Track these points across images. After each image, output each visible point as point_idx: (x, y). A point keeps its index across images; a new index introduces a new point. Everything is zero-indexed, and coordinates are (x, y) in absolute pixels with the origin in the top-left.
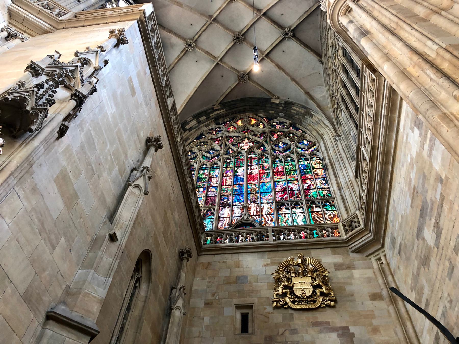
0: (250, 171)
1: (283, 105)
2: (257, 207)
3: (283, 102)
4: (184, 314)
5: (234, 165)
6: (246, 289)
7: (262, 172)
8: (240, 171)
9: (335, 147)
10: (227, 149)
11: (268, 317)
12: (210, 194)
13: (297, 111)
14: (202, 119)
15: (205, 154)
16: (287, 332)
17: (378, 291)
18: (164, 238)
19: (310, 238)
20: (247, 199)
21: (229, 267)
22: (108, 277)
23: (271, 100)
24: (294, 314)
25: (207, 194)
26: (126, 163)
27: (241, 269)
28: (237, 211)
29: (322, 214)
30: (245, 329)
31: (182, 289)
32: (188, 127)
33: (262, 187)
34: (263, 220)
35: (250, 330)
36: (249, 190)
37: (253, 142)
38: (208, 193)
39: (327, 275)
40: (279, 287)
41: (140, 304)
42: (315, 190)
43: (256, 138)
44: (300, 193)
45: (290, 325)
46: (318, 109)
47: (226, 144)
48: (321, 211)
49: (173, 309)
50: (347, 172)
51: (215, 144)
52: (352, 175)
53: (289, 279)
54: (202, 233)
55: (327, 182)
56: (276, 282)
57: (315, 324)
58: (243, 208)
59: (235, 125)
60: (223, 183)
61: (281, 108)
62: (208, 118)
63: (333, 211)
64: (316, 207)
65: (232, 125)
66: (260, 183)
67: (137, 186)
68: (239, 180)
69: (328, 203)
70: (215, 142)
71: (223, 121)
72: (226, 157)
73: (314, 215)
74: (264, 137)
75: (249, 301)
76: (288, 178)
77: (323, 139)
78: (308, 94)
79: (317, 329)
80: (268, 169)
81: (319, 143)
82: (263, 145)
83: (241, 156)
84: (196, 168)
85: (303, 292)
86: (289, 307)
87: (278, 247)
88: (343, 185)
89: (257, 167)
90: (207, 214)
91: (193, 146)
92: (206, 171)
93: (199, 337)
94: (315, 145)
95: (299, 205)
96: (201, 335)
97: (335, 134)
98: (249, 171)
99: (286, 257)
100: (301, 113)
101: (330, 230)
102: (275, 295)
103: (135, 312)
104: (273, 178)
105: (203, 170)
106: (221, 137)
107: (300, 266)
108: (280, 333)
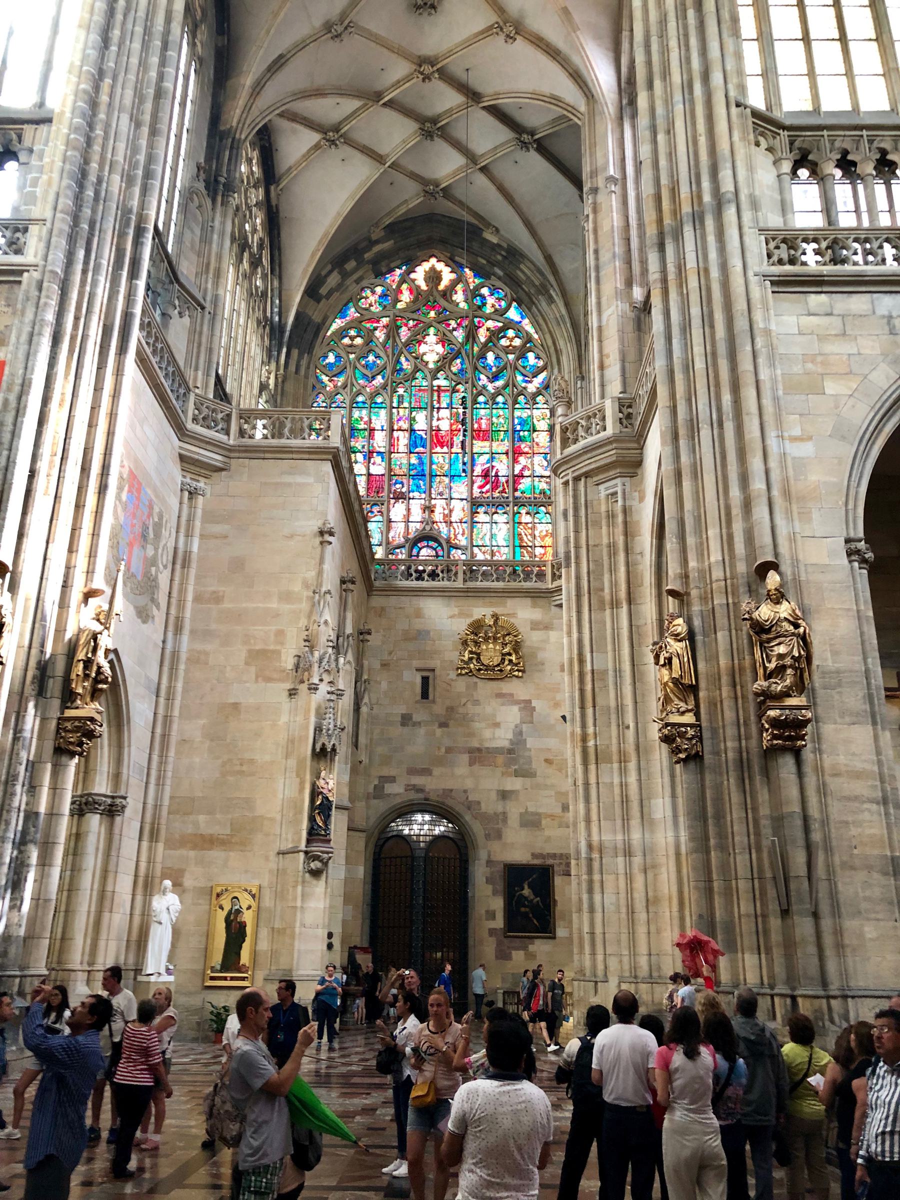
1: (503, 253)
5: (410, 403)
7: (454, 427)
13: (528, 278)
21: (407, 617)
30: (425, 695)
32: (323, 291)
38: (371, 466)
57: (500, 695)
61: (499, 258)
62: (360, 263)
64: (527, 513)
68: (418, 441)
69: (542, 508)
71: (388, 265)
73: (521, 530)
75: (430, 664)
78: (549, 259)
79: (499, 700)
92: (364, 412)
94: (544, 368)
98: (435, 423)
100: (534, 285)
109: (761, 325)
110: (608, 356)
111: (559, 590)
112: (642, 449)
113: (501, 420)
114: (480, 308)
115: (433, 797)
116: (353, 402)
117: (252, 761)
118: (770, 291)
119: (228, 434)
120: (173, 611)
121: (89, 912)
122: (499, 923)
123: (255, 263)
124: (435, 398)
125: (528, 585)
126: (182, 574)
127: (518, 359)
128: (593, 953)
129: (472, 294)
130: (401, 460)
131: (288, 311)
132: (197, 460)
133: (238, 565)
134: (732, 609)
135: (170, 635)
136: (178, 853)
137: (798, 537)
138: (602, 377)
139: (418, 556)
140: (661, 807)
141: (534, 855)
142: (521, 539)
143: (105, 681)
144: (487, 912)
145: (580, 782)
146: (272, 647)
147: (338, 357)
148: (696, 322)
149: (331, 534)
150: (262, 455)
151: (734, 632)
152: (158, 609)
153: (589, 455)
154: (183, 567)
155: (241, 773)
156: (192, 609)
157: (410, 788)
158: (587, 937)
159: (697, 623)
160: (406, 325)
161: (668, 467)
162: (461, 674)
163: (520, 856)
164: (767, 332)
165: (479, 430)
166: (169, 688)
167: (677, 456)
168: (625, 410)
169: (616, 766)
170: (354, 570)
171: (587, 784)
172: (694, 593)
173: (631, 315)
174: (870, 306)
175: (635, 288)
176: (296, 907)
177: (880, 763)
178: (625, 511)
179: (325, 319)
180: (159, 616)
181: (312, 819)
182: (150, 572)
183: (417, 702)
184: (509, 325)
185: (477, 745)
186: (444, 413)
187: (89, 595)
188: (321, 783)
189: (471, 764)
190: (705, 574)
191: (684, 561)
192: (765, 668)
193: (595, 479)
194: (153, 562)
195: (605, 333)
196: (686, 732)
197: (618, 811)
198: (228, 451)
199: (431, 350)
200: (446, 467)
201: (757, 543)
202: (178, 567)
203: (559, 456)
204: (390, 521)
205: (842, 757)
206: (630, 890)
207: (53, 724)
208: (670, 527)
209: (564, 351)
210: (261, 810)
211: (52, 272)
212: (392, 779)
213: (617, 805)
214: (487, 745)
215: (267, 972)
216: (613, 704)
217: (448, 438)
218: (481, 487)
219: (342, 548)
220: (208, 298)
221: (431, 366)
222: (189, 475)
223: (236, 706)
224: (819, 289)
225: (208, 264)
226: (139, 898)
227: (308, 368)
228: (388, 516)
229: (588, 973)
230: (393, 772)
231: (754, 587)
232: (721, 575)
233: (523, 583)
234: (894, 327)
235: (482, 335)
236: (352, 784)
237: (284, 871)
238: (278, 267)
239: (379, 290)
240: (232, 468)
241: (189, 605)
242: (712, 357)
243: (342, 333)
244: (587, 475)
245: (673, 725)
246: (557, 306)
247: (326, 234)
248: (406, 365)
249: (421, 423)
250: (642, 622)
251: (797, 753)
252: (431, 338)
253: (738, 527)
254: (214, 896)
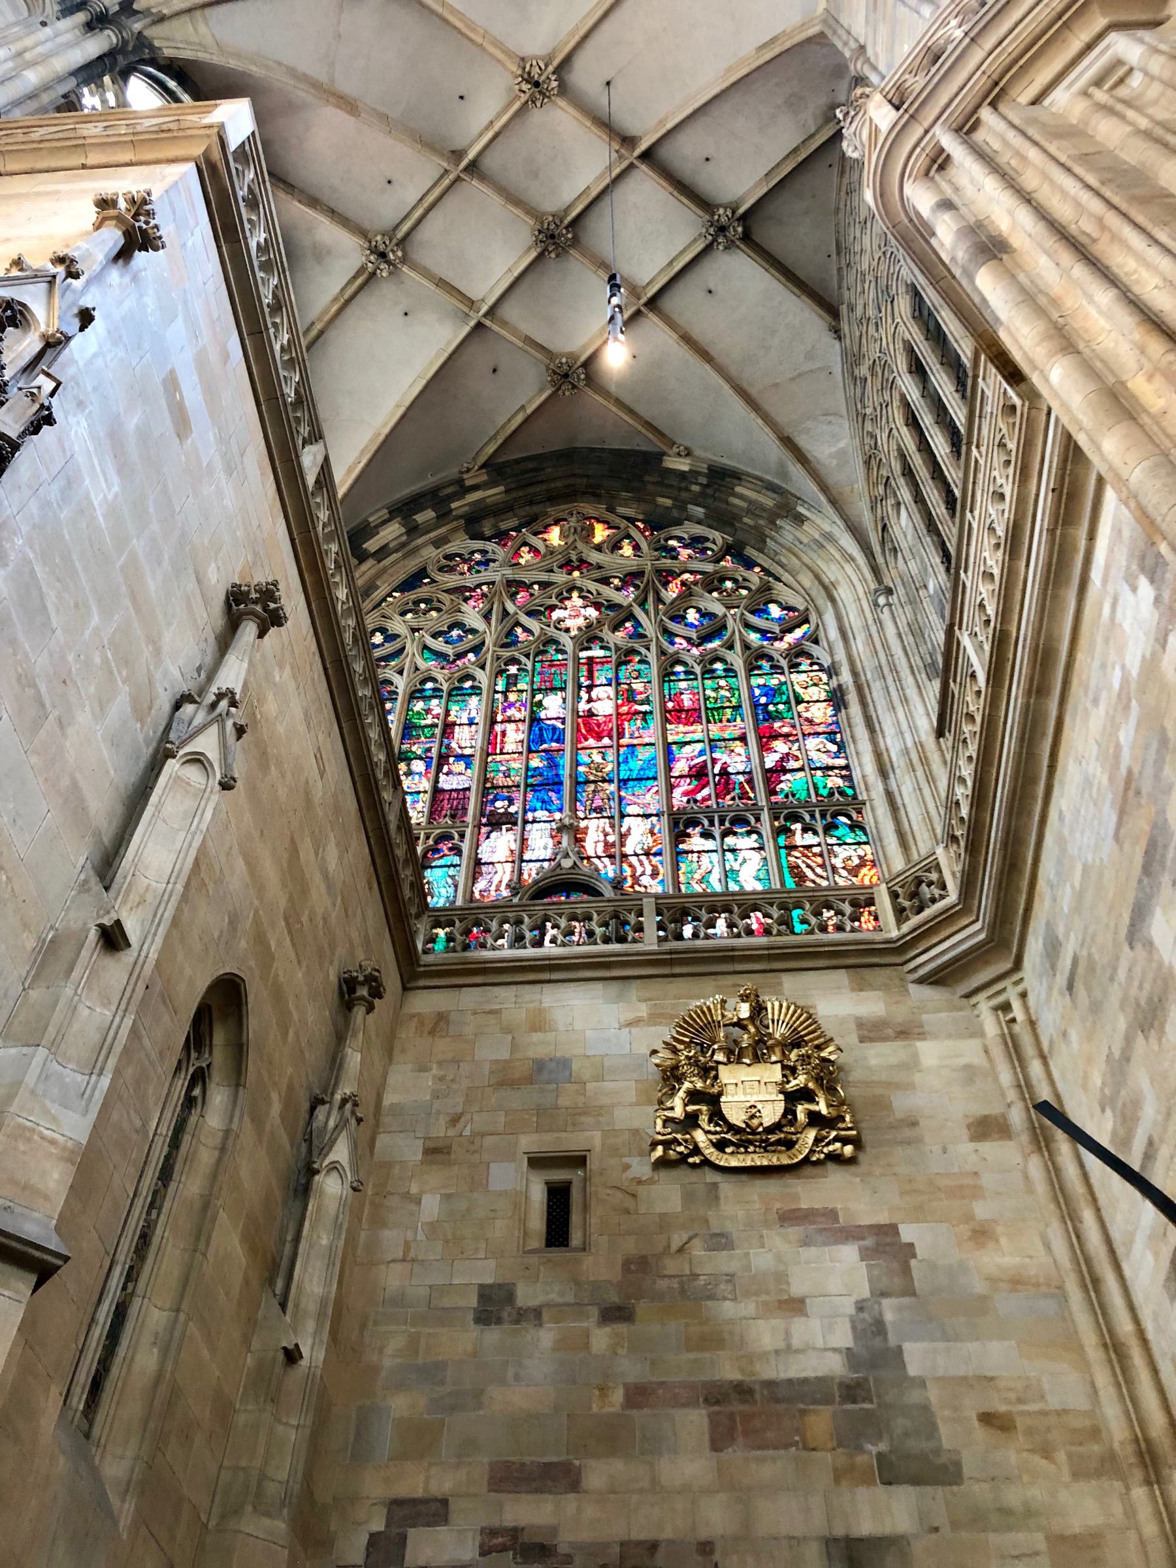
0: (587, 707)
1: (704, 480)
2: (608, 829)
3: (703, 468)
4: (355, 1189)
5: (533, 682)
6: (563, 1101)
7: (625, 709)
8: (553, 706)
9: (873, 629)
10: (508, 626)
11: (634, 1196)
12: (446, 783)
13: (751, 502)
14: (420, 518)
15: (430, 641)
16: (696, 1242)
17: (994, 1109)
18: (290, 932)
19: (779, 934)
20: (574, 799)
21: (508, 1030)
22: (96, 1071)
23: (661, 461)
24: (721, 1186)
25: (437, 781)
26: (158, 675)
27: (550, 1036)
28: (541, 843)
29: (821, 855)
30: (557, 1232)
31: (349, 1106)
32: (372, 545)
33: (626, 761)
34: (628, 871)
35: (576, 1238)
36: (581, 769)
37: (597, 606)
38: (442, 777)
39: (832, 1058)
40: (672, 1095)
41: (206, 1157)
42: (802, 774)
43: (608, 592)
44: (750, 782)
45: (707, 1222)
46: (823, 498)
47: (505, 610)
48: (819, 845)
49: (318, 1172)
50: (910, 716)
51: (465, 607)
52: (925, 724)
53: (708, 1071)
54: (418, 916)
55: (841, 747)
56: (665, 1079)
57: (789, 1217)
58: (559, 830)
59: (536, 541)
60: (492, 744)
62: (444, 516)
63: (859, 843)
64: (805, 830)
65: (525, 544)
66: (619, 746)
67: (197, 759)
69: (843, 819)
70: (466, 600)
71: (495, 526)
72: (506, 654)
73: (797, 858)
74: (637, 587)
75: (572, 1142)
76: (715, 731)
77: (833, 600)
78: (788, 442)
80: (647, 701)
81: (820, 614)
82: (631, 616)
83: (558, 651)
84: (400, 691)
85: (753, 1112)
86: (706, 1162)
87: (676, 964)
88: (894, 759)
89: (610, 691)
90: (437, 851)
91: (389, 612)
92: (435, 702)
93: (404, 1260)
94: (806, 621)
95: (748, 823)
96: (412, 1255)
97: (873, 586)
98: (583, 707)
99: (699, 999)
100: (764, 509)
101: (847, 909)
102: (659, 1122)
103: (189, 1185)
104: (664, 731)
105: (424, 698)
106: (487, 584)
107: (744, 1028)
108: (675, 1246)
165: (679, 709)
185: (729, 1372)
189: (717, 1445)
204: (478, 863)
214: (769, 1372)
247: (372, 440)
249: (553, 706)
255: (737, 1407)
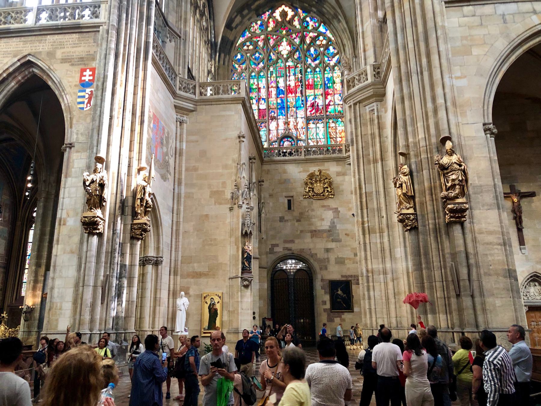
5: (276, 74)
25: (259, 107)
30: (289, 208)
32: (234, 25)
35: (292, 208)
42: (333, 106)
57: (323, 206)
61: (314, 3)
62: (250, 10)
64: (333, 122)
68: (281, 92)
69: (340, 120)
73: (330, 130)
79: (324, 209)
92: (255, 80)
98: (288, 83)
109: (440, 24)
110: (367, 45)
111: (349, 157)
112: (385, 88)
113: (319, 80)
114: (306, 27)
115: (295, 252)
116: (250, 76)
117: (215, 239)
118: (444, 7)
119: (195, 94)
120: (177, 176)
121: (150, 306)
122: (328, 306)
123: (202, 14)
124: (288, 71)
125: (334, 155)
126: (180, 159)
127: (325, 50)
128: (371, 317)
129: (302, 21)
130: (273, 100)
131: (218, 36)
132: (182, 107)
133: (203, 153)
134: (430, 160)
135: (176, 186)
136: (186, 280)
137: (460, 124)
138: (365, 55)
139: (283, 145)
140: (399, 252)
141: (342, 276)
142: (330, 135)
143: (150, 207)
144: (323, 301)
145: (362, 243)
146: (221, 189)
147: (242, 56)
148: (409, 25)
149: (244, 137)
150: (210, 103)
151: (431, 170)
152: (170, 174)
153: (360, 93)
154: (180, 156)
155: (211, 244)
156: (185, 175)
157: (285, 249)
158: (368, 311)
159: (413, 167)
160: (272, 38)
161: (397, 95)
162: (305, 198)
163: (336, 277)
164: (443, 27)
165: (309, 85)
166: (178, 209)
167: (402, 90)
168: (377, 70)
169: (378, 235)
170: (255, 154)
171: (365, 244)
172: (412, 153)
173: (378, 25)
174: (494, 10)
175: (379, 12)
176: (238, 302)
177: (502, 227)
178: (378, 117)
179: (235, 38)
180: (171, 178)
181: (243, 263)
182: (165, 158)
183: (286, 211)
184: (320, 34)
185: (314, 229)
186: (292, 78)
187: (140, 170)
188: (246, 247)
190: (416, 144)
191: (407, 139)
192: (446, 186)
193: (364, 104)
194: (167, 154)
195: (365, 35)
196: (410, 217)
197: (380, 255)
198: (196, 102)
199: (285, 48)
200: (294, 104)
201: (441, 128)
202: (177, 156)
203: (346, 94)
204: (270, 130)
205: (483, 225)
206: (386, 289)
207: (129, 226)
208: (400, 123)
209: (346, 45)
210: (221, 260)
211: (112, 25)
212: (277, 245)
213: (379, 252)
214: (319, 229)
215: (227, 329)
216: (375, 206)
217: (294, 90)
218: (311, 111)
219: (249, 143)
220: (182, 33)
221: (285, 56)
222: (179, 115)
223: (207, 216)
224: (469, 4)
225: (181, 17)
226: (171, 300)
227: (229, 61)
228: (269, 128)
229: (369, 326)
230: (277, 242)
231: (440, 149)
232: (424, 144)
233: (332, 155)
234: (506, 20)
235: (308, 41)
236: (259, 248)
237: (233, 286)
238: (212, 15)
239: (259, 22)
240: (198, 110)
241: (183, 173)
242: (416, 42)
243: (243, 44)
244: (360, 102)
245: (404, 214)
246: (342, 24)
248: (273, 57)
250: (388, 169)
251: (462, 224)
252: (284, 43)
253: (431, 121)
254: (203, 298)
255: (314, 233)
